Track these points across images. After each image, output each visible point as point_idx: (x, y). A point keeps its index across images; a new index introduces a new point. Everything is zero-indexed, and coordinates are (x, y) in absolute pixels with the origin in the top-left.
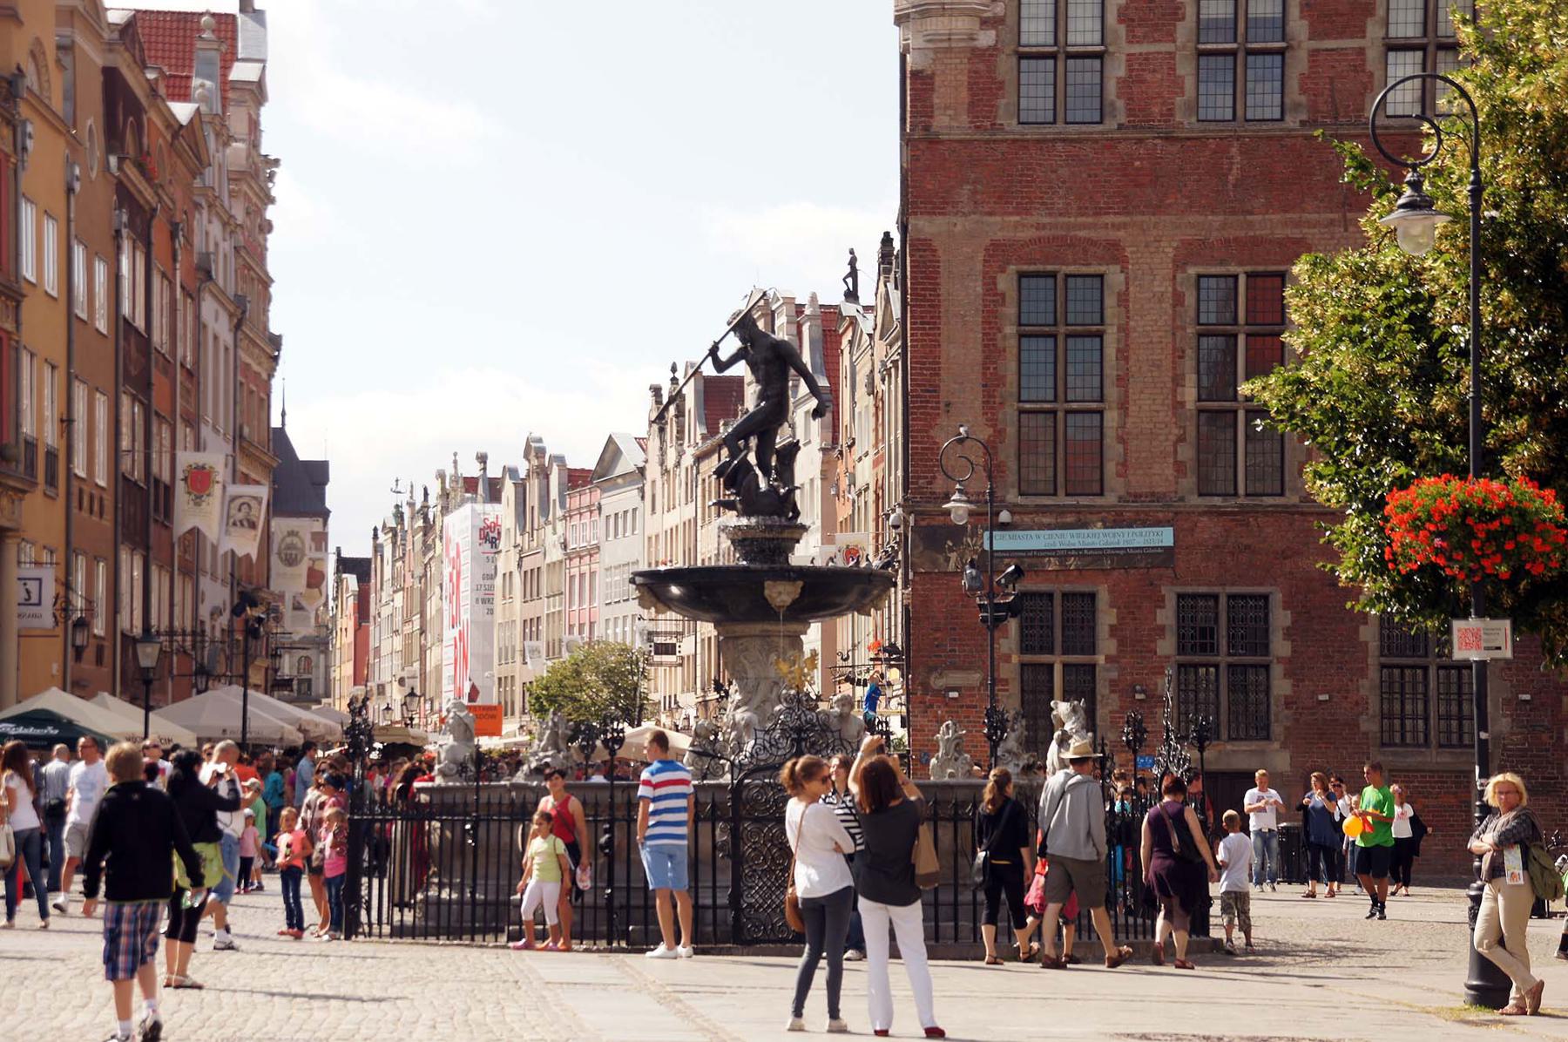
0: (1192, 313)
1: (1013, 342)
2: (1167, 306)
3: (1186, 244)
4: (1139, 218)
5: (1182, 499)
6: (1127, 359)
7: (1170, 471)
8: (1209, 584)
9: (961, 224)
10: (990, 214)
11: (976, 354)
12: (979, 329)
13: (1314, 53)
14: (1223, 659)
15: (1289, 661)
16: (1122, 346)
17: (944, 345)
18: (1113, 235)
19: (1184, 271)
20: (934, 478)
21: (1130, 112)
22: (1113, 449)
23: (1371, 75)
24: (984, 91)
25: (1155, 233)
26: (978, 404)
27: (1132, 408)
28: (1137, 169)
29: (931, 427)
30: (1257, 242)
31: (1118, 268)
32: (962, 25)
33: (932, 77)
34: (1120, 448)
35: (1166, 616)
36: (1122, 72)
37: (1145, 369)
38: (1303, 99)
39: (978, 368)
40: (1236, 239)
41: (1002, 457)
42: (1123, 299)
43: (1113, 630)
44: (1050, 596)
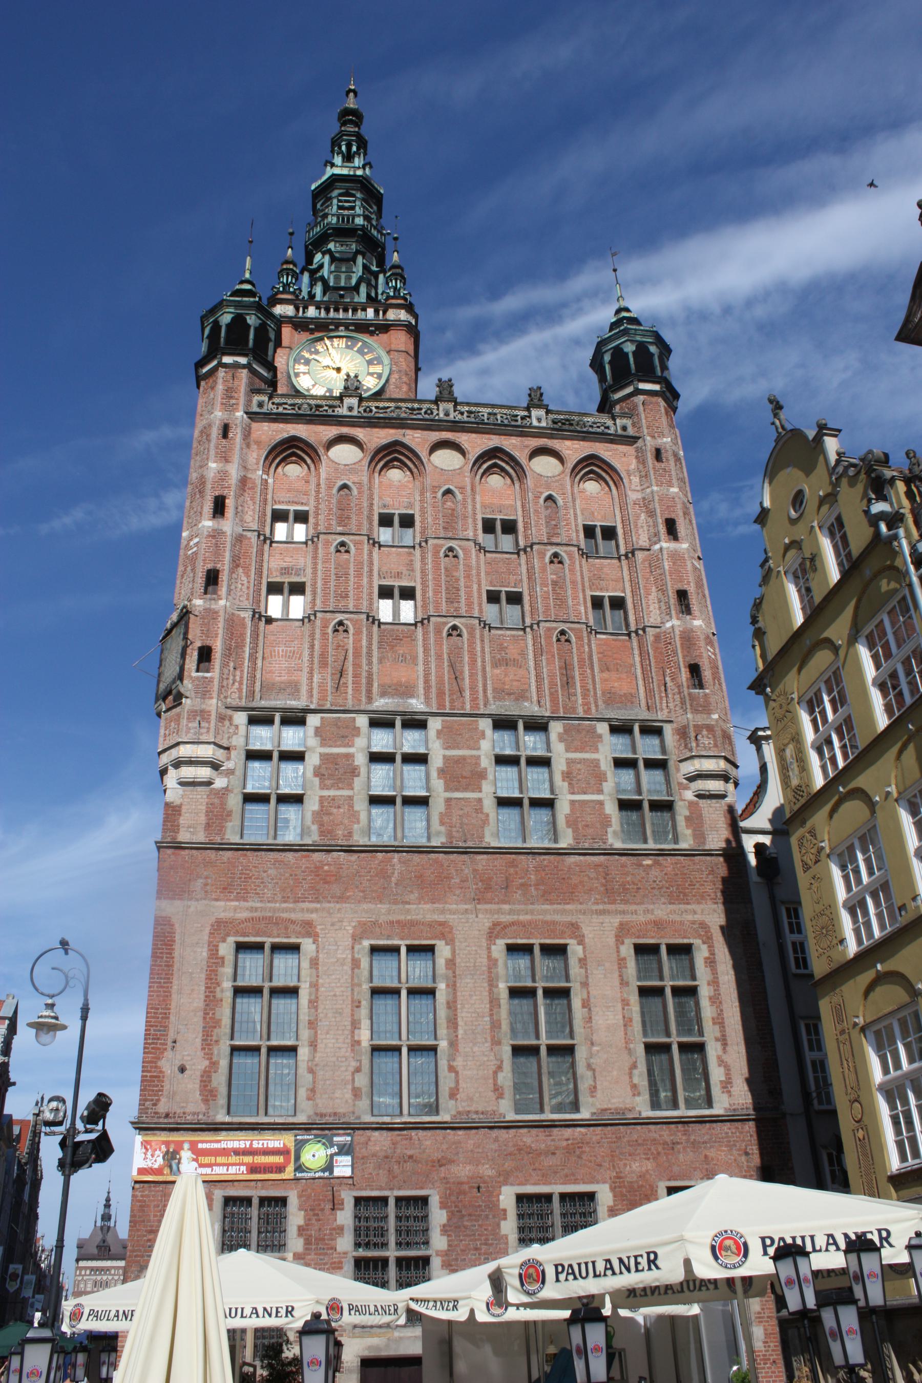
0: (366, 973)
1: (229, 994)
2: (347, 968)
3: (361, 924)
4: (327, 905)
5: (359, 1118)
6: (316, 1008)
7: (349, 1095)
8: (381, 1189)
9: (194, 906)
10: (217, 900)
11: (198, 1001)
12: (203, 983)
14: (392, 1253)
15: (445, 1254)
16: (313, 997)
17: (174, 996)
18: (308, 916)
19: (360, 944)
20: (158, 1100)
21: (322, 833)
22: (305, 1078)
23: (487, 815)
24: (217, 816)
25: (339, 915)
26: (199, 1041)
27: (320, 1046)
28: (326, 871)
29: (159, 1059)
30: (413, 924)
31: (311, 940)
32: (204, 773)
33: (180, 806)
34: (310, 1077)
35: (345, 1217)
36: (316, 807)
37: (330, 1015)
38: (442, 829)
39: (201, 1014)
40: (398, 922)
41: (214, 1084)
42: (314, 963)
43: (301, 1230)
44: (248, 1201)
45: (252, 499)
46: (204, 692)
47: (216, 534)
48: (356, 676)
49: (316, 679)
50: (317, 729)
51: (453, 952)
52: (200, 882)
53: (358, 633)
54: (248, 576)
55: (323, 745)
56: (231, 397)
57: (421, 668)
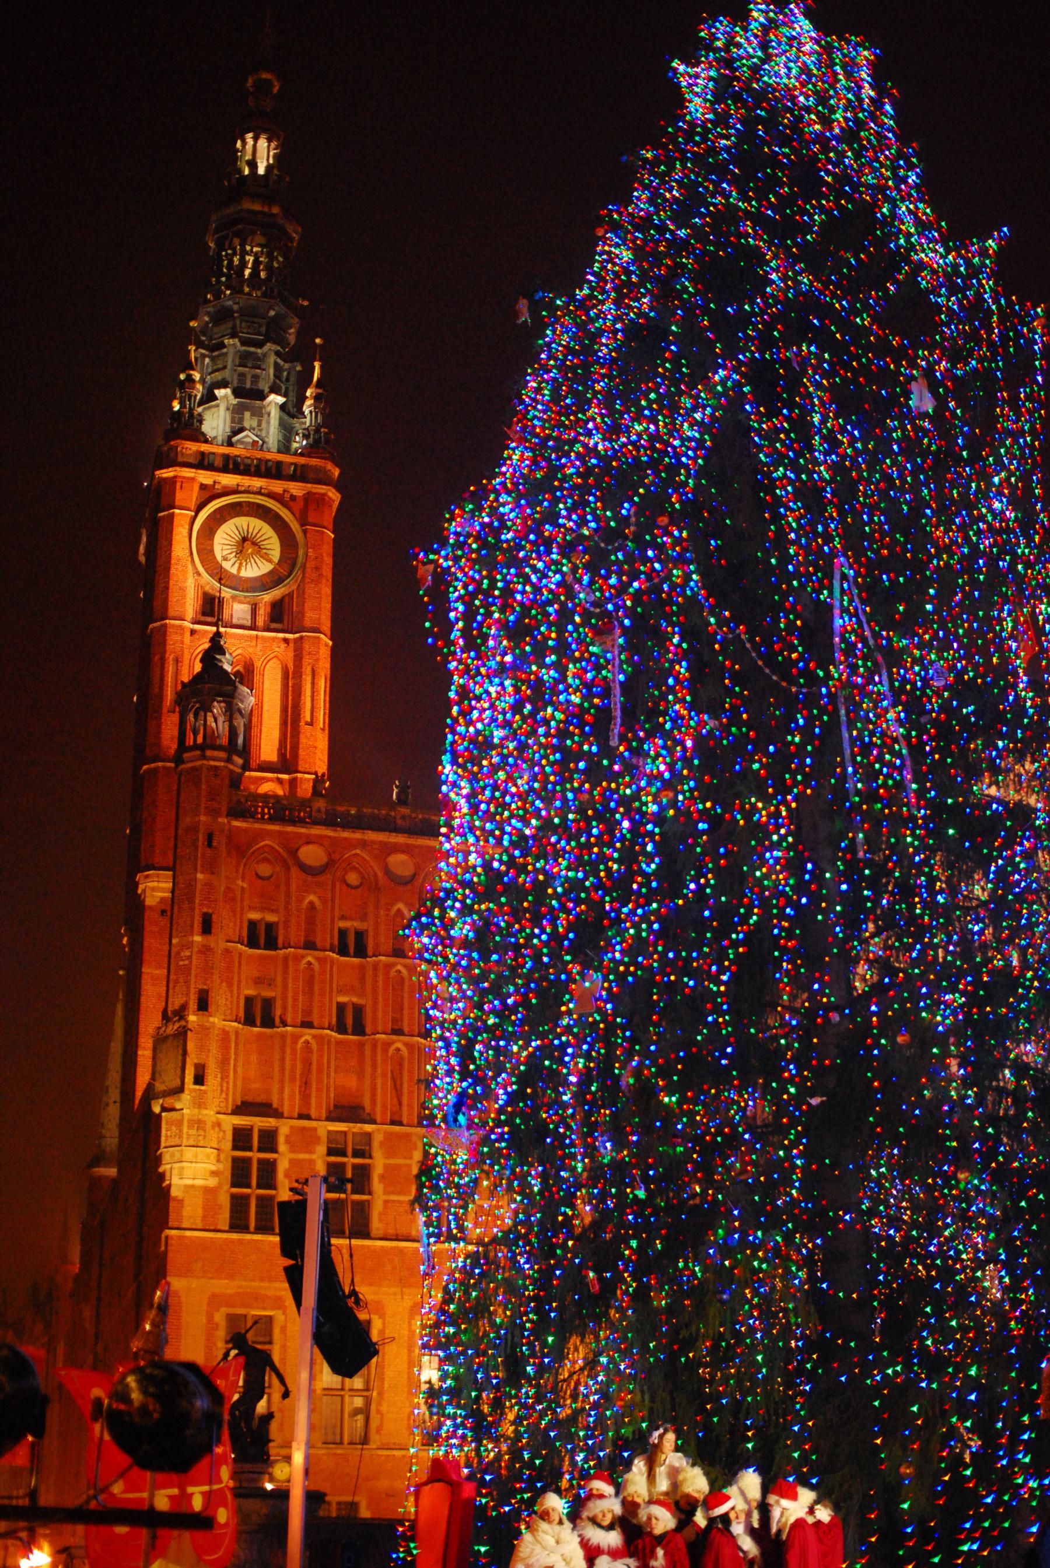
9: (195, 1283)
13: (386, 1202)
18: (278, 1294)
31: (280, 1312)
42: (284, 1329)
45: (234, 911)
46: (200, 1103)
47: (206, 950)
48: (319, 1090)
49: (287, 1091)
50: (287, 1136)
51: (384, 1324)
52: (199, 1265)
53: (320, 1050)
54: (231, 991)
55: (292, 1151)
56: (213, 799)
57: (367, 1082)
